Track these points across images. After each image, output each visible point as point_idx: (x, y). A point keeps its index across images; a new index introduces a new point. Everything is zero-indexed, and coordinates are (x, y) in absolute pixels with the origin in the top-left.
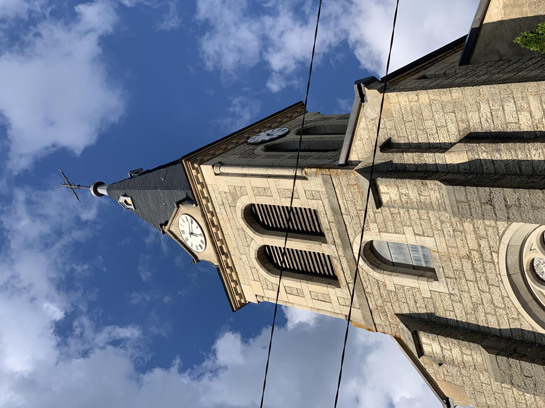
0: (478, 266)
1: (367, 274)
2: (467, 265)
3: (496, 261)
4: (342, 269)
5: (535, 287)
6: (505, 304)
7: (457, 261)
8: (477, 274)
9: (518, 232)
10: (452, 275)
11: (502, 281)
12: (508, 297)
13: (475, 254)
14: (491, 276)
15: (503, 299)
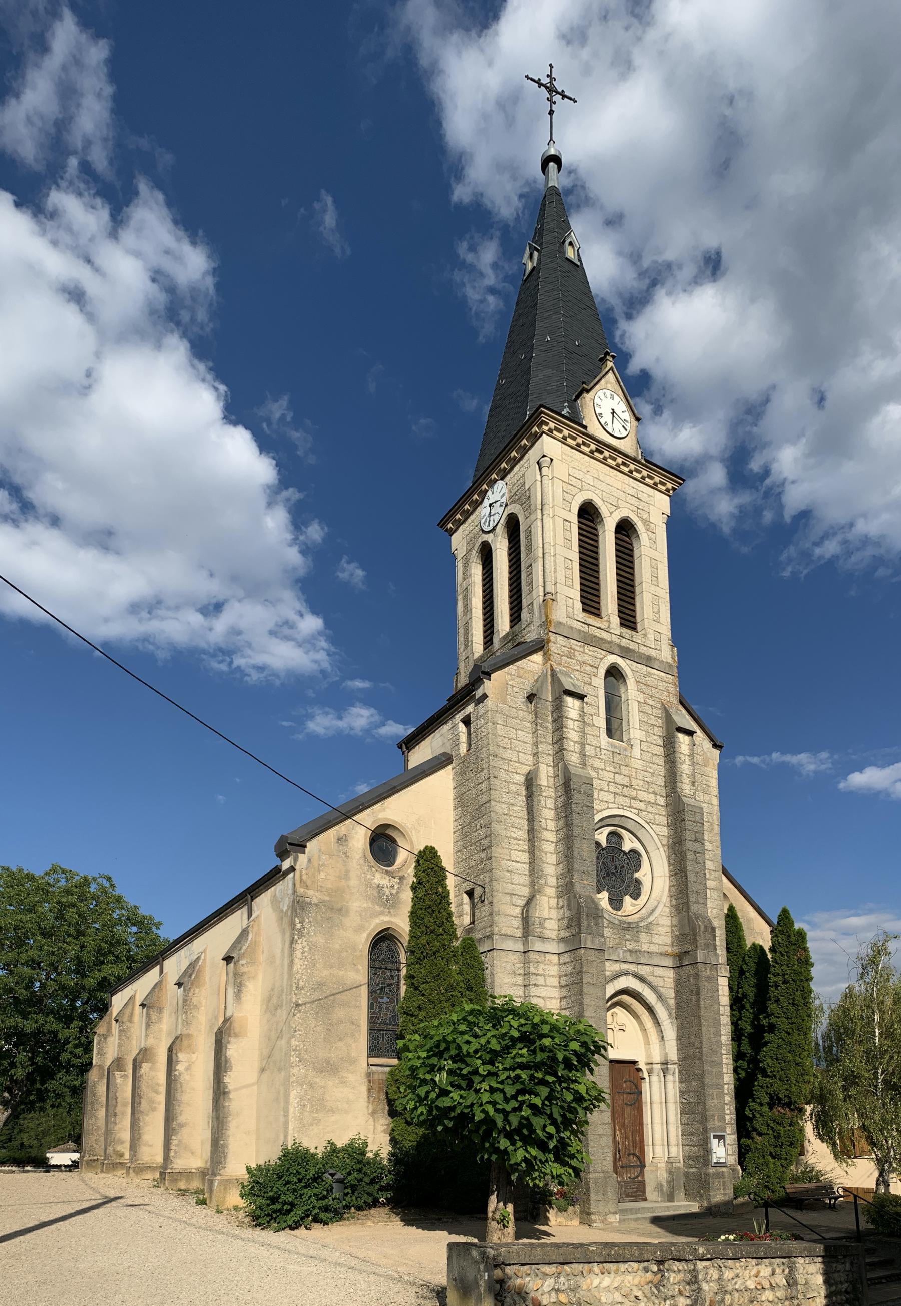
0: (626, 791)
1: (601, 659)
2: (626, 781)
3: (632, 810)
4: (600, 628)
5: (607, 830)
6: (602, 801)
7: (627, 772)
8: (620, 787)
9: (651, 839)
10: (616, 760)
11: (618, 808)
12: (608, 808)
13: (633, 794)
14: (620, 800)
15: (606, 802)
